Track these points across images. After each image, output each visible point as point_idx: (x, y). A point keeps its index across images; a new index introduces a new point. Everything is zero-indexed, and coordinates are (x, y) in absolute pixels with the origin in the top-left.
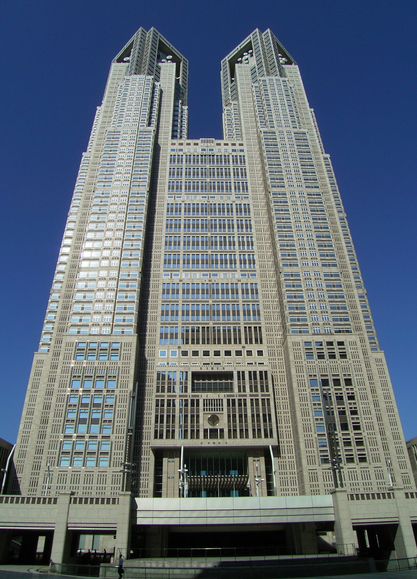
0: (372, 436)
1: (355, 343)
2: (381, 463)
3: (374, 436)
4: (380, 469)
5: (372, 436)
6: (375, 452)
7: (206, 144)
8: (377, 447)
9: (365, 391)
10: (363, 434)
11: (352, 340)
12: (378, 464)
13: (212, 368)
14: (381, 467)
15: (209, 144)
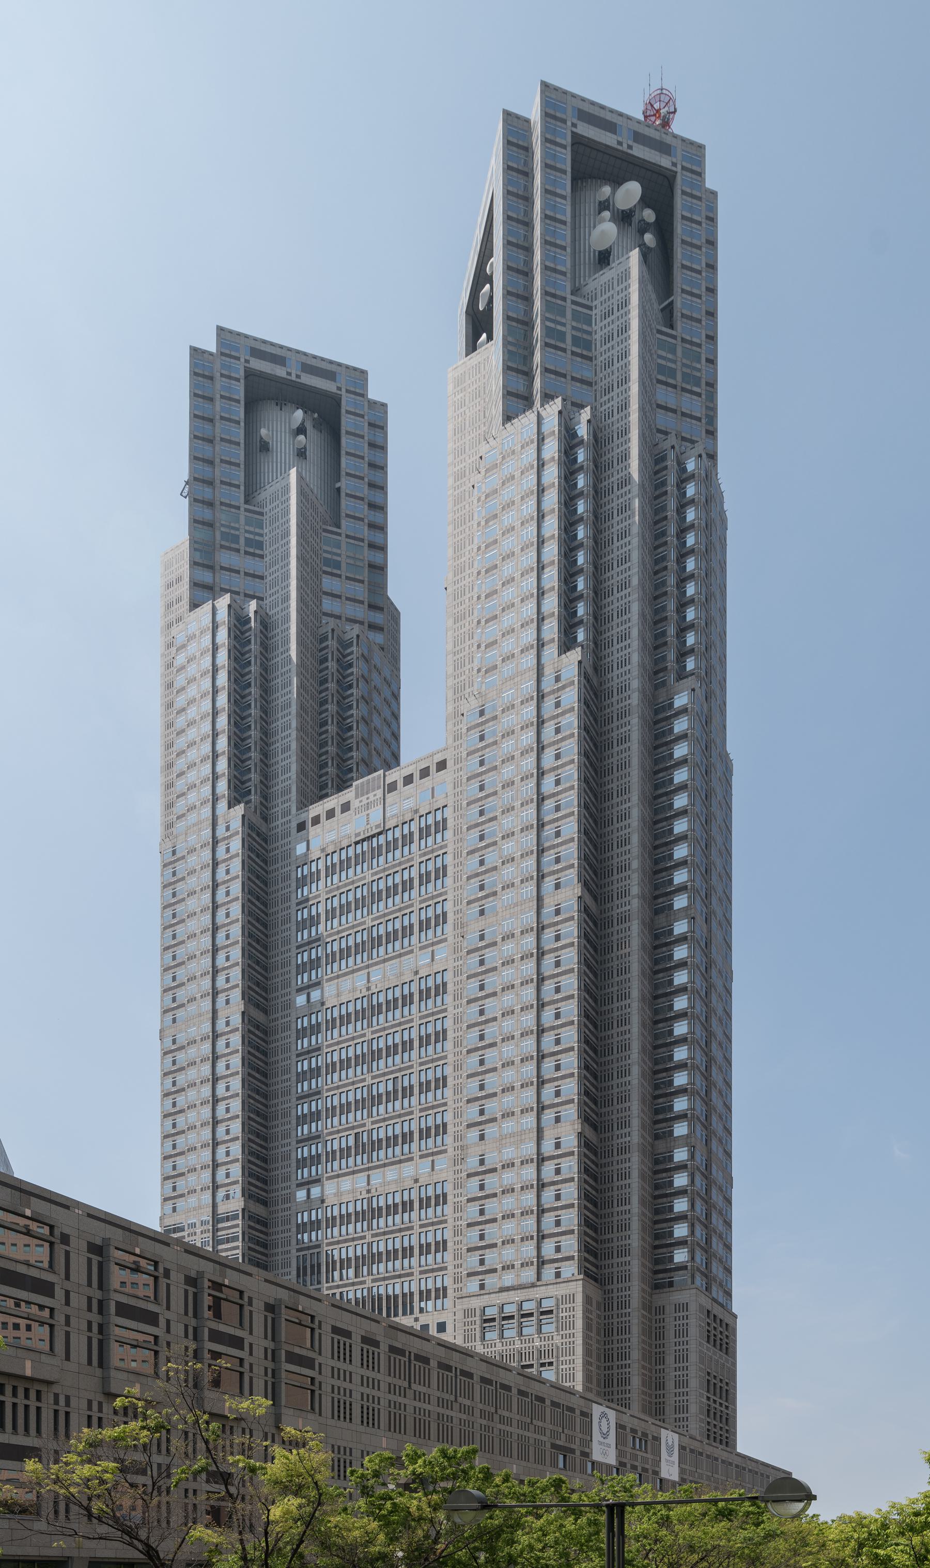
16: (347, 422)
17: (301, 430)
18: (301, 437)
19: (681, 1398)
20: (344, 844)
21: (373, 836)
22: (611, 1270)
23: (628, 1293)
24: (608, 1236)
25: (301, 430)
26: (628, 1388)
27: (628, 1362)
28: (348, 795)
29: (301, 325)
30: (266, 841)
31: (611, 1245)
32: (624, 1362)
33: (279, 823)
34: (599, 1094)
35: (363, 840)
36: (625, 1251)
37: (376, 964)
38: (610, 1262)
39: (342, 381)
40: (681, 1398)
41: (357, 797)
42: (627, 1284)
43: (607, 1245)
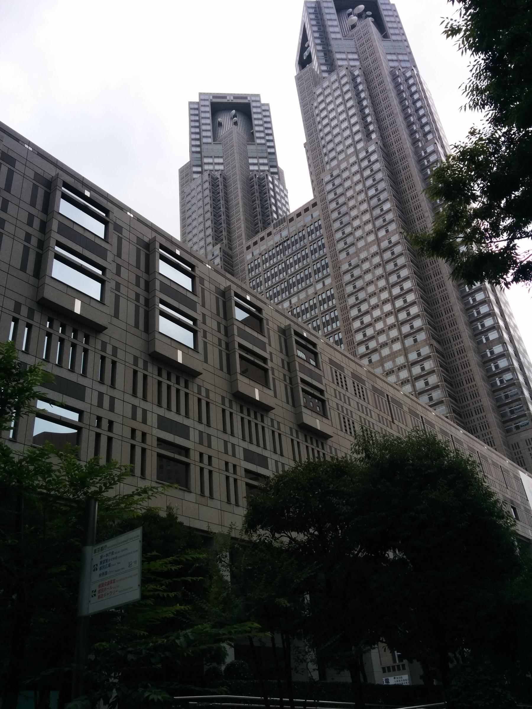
7: (278, 228)
15: (281, 226)
16: (254, 110)
17: (235, 116)
18: (235, 118)
20: (271, 249)
23: (490, 436)
24: (465, 403)
25: (235, 116)
28: (270, 229)
29: (231, 85)
30: (232, 258)
31: (469, 408)
33: (237, 249)
34: (436, 325)
35: (280, 245)
36: (480, 410)
37: (294, 295)
38: (472, 418)
39: (249, 98)
41: (274, 228)
42: (488, 431)
43: (466, 409)
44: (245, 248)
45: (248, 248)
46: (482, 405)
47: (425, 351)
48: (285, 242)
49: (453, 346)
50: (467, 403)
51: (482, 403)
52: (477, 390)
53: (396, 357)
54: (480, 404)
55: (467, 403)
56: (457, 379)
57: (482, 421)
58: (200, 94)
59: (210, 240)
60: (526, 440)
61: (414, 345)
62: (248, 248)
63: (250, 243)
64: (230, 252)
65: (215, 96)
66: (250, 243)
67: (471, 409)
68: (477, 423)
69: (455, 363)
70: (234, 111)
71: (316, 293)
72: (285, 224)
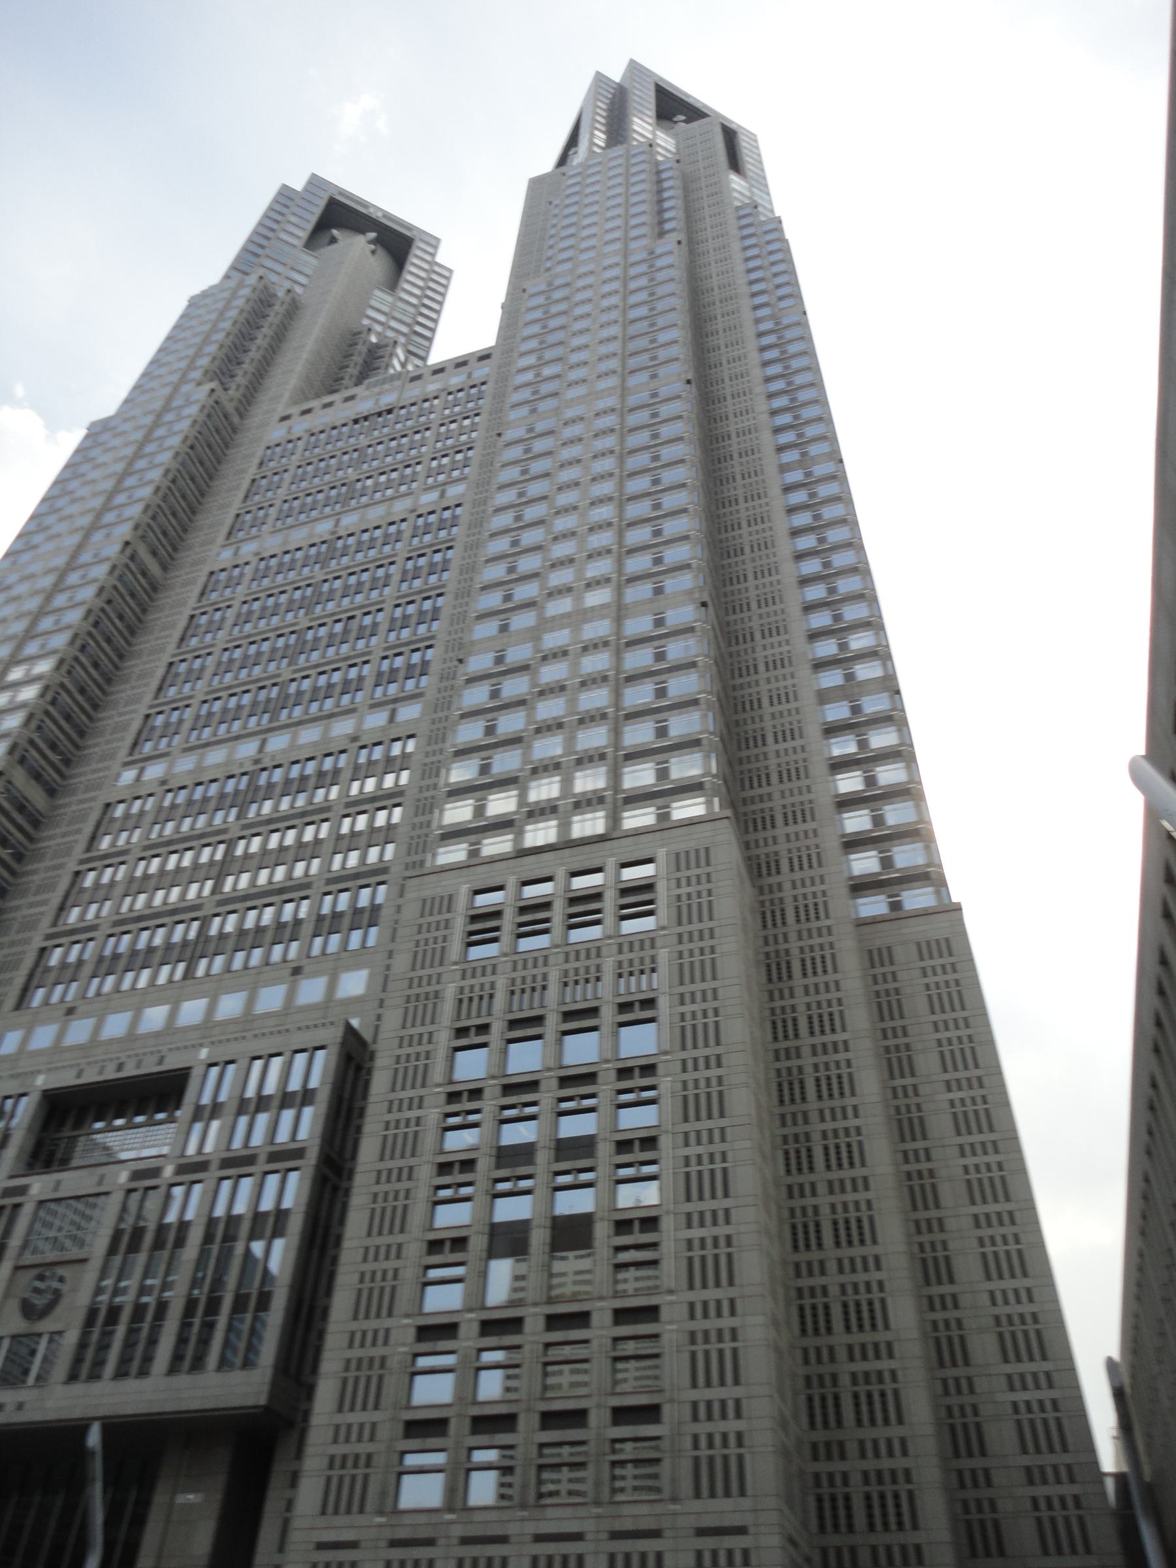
0: (713, 1324)
1: (705, 855)
2: (746, 1503)
3: (726, 1322)
4: (736, 1543)
5: (713, 1324)
6: (718, 1427)
7: (376, 390)
8: (738, 1392)
9: (714, 1073)
10: (664, 1314)
11: (691, 845)
12: (723, 1510)
13: (120, 1067)
14: (741, 1531)
15: (387, 386)
19: (981, 1159)
21: (380, 414)
22: (771, 849)
24: (758, 791)
26: (849, 1101)
27: (840, 1037)
31: (767, 805)
32: (829, 1038)
35: (366, 418)
38: (769, 834)
40: (981, 1159)
43: (757, 807)
44: (277, 417)
45: (285, 418)
46: (811, 802)
47: (682, 614)
48: (380, 414)
49: (759, 649)
50: (765, 790)
51: (812, 796)
52: (805, 760)
53: (585, 621)
54: (806, 797)
55: (765, 790)
56: (750, 727)
57: (803, 843)
58: (314, 176)
59: (196, 375)
60: (918, 944)
61: (651, 601)
62: (285, 418)
63: (295, 410)
64: (236, 419)
65: (343, 193)
66: (295, 410)
67: (771, 809)
68: (782, 847)
69: (753, 690)
70: (372, 235)
71: (413, 511)
72: (397, 383)
